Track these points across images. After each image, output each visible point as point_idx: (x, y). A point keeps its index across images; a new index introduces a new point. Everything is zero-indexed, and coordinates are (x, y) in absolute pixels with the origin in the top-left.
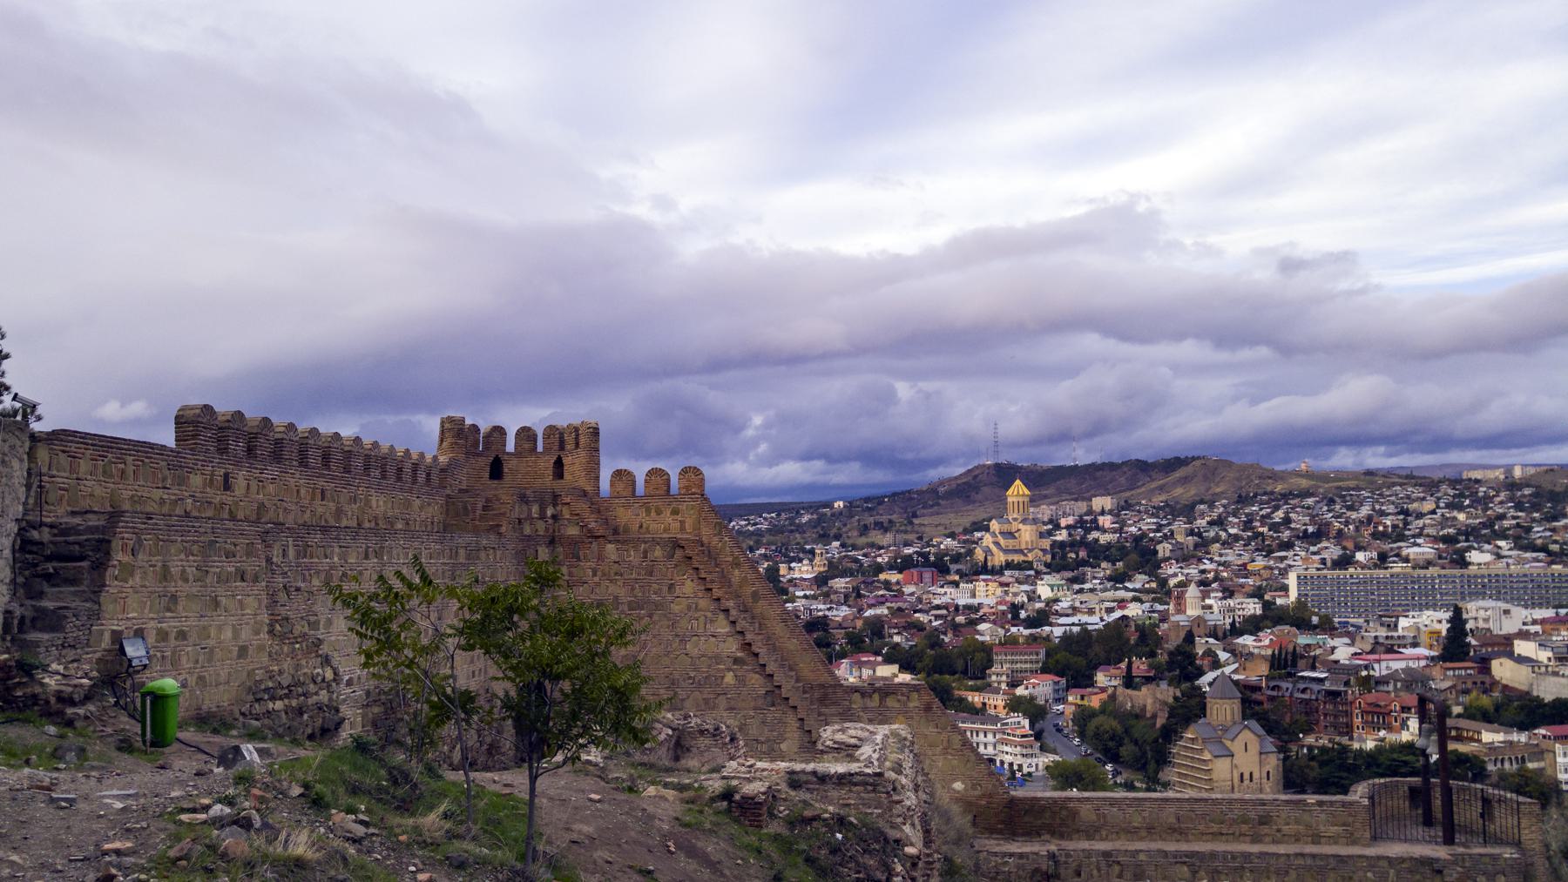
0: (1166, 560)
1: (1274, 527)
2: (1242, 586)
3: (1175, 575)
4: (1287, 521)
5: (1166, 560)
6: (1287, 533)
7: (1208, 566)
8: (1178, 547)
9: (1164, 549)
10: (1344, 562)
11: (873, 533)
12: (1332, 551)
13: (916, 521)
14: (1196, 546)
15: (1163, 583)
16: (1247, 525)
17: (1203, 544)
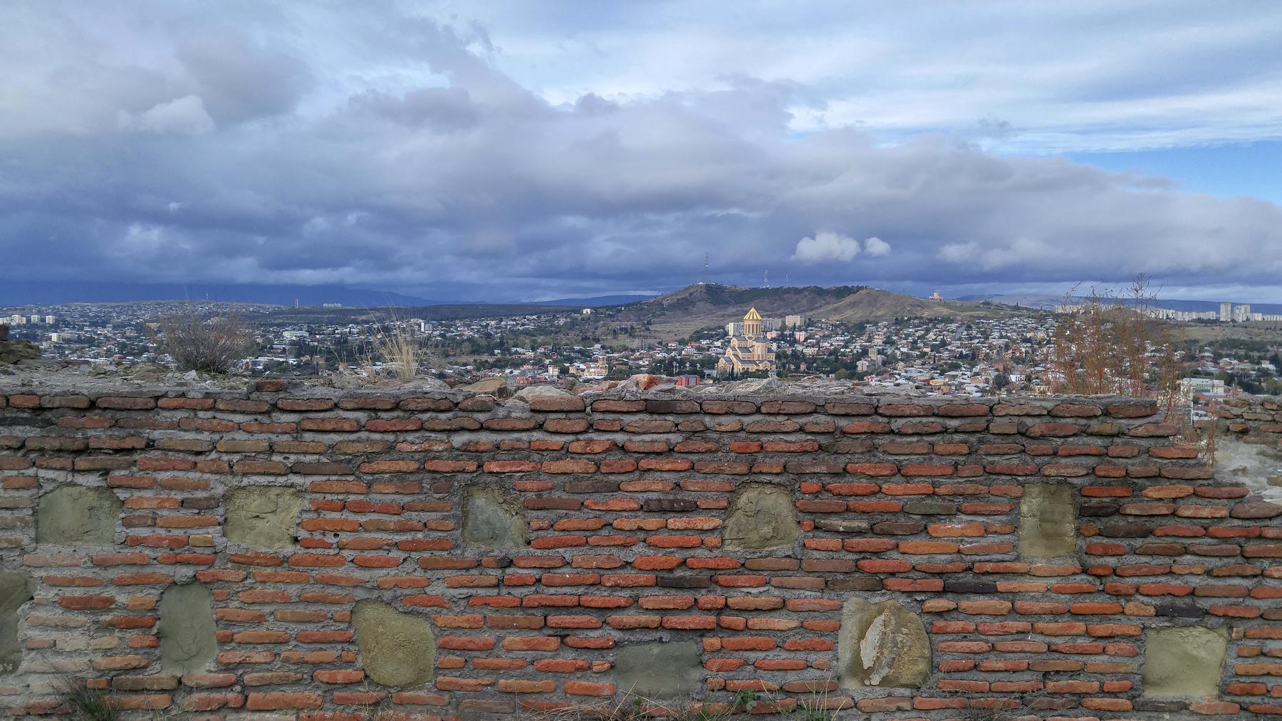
0: (867, 374)
1: (934, 348)
4: (944, 344)
5: (867, 374)
6: (946, 354)
8: (873, 363)
9: (862, 365)
11: (621, 337)
13: (651, 328)
14: (884, 363)
16: (914, 346)
17: (889, 361)
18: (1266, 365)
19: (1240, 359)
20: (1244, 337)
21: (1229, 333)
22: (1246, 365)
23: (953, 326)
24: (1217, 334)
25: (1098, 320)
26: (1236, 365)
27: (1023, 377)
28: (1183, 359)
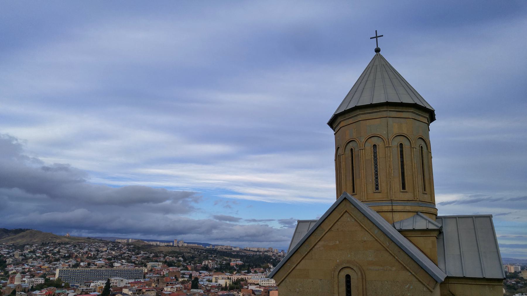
1: (54, 254)
2: (38, 274)
3: (12, 270)
4: (59, 252)
6: (58, 256)
7: (26, 266)
8: (16, 260)
9: (9, 261)
10: (77, 265)
12: (73, 262)
14: (23, 260)
15: (7, 273)
16: (44, 253)
17: (25, 259)
18: (181, 259)
19: (173, 257)
20: (178, 250)
21: (173, 249)
22: (174, 259)
23: (68, 246)
24: (170, 249)
25: (128, 244)
26: (169, 259)
27: (87, 263)
28: (153, 257)
